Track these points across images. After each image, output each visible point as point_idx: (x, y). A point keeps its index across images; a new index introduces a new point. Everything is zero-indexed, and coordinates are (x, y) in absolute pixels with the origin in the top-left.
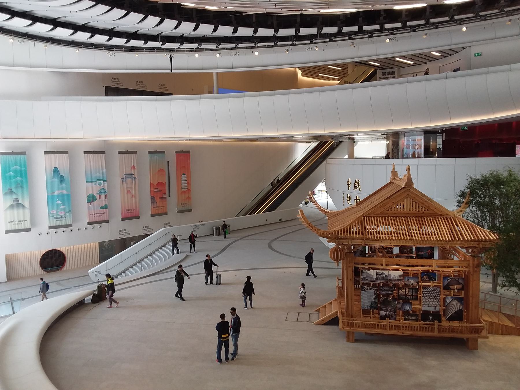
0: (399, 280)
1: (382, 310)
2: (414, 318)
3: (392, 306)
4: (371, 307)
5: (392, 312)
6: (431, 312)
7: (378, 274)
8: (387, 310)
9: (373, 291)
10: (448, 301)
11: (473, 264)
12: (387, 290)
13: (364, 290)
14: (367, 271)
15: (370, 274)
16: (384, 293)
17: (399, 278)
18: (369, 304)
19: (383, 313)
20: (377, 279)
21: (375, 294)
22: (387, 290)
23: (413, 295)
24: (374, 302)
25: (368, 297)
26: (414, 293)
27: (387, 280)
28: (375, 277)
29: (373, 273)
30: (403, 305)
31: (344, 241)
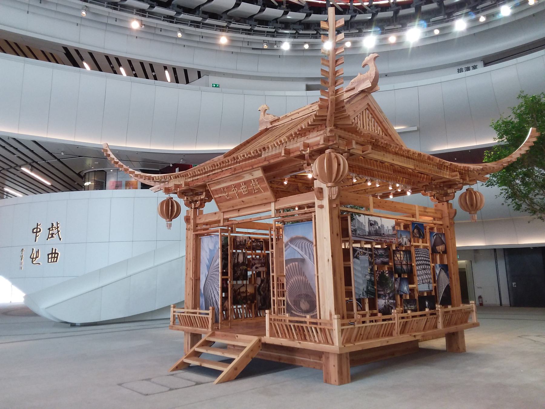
0: (394, 235)
1: (379, 296)
2: (413, 307)
3: (390, 288)
4: (368, 292)
5: (390, 298)
6: (425, 294)
7: (371, 224)
8: (385, 296)
9: (366, 258)
10: (437, 272)
11: (449, 213)
12: (381, 256)
13: (356, 257)
14: (357, 216)
15: (362, 223)
16: (379, 261)
17: (391, 233)
18: (365, 286)
19: (381, 303)
20: (370, 234)
21: (371, 263)
22: (381, 256)
23: (408, 265)
24: (370, 281)
25: (360, 271)
26: (408, 259)
27: (380, 235)
28: (367, 229)
29: (363, 220)
30: (400, 284)
31: (341, 141)
